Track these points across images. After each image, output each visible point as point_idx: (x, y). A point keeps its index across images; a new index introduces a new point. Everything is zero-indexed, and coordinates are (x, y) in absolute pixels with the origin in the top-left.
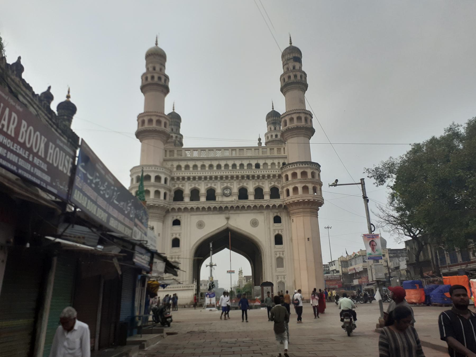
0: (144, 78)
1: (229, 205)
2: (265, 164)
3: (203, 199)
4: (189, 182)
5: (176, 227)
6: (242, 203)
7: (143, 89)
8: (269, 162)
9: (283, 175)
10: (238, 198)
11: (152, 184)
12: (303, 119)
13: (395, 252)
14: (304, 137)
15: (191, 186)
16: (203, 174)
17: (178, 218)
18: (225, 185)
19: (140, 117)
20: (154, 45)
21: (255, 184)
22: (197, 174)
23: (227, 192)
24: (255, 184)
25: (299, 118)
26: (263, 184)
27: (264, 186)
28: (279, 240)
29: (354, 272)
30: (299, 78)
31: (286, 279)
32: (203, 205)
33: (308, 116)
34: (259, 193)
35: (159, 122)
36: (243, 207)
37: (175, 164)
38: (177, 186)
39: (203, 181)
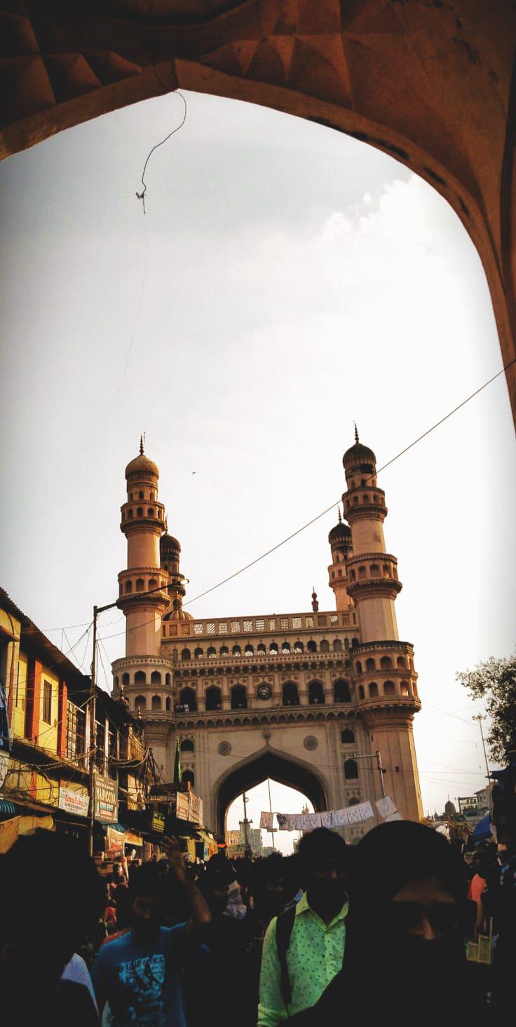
0: (125, 511)
1: (269, 715)
2: (324, 642)
6: (288, 710)
7: (124, 528)
17: (189, 737)
18: (261, 680)
19: (122, 576)
24: (309, 677)
25: (374, 568)
26: (321, 676)
27: (323, 680)
32: (226, 717)
34: (316, 690)
38: (184, 686)
39: (225, 675)
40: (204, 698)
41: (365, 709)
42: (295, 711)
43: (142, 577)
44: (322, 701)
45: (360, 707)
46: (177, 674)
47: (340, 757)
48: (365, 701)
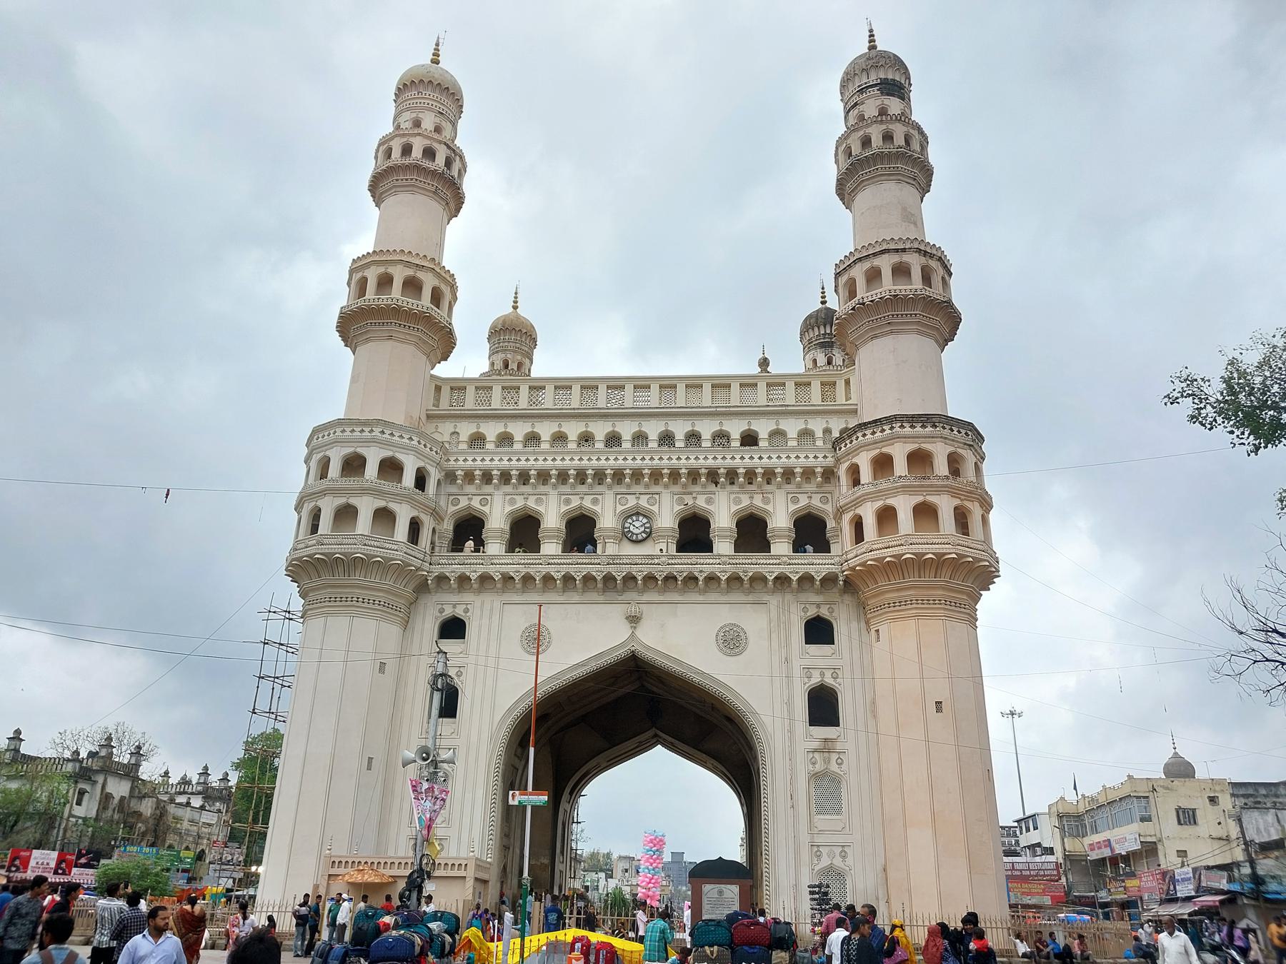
0: (380, 154)
1: (640, 572)
2: (778, 434)
3: (551, 548)
4: (508, 489)
5: (450, 645)
7: (379, 187)
8: (792, 427)
9: (842, 471)
11: (367, 485)
12: (916, 273)
13: (1251, 791)
15: (512, 502)
16: (553, 463)
17: (459, 612)
18: (632, 501)
20: (426, 59)
22: (534, 463)
23: (637, 527)
25: (901, 271)
27: (769, 508)
28: (823, 707)
29: (1106, 853)
30: (899, 140)
31: (849, 861)
32: (545, 569)
33: (934, 264)
34: (752, 532)
35: (413, 286)
37: (466, 429)
38: (464, 502)
40: (502, 531)
43: (391, 270)
44: (764, 546)
45: (852, 563)
47: (797, 672)
48: (863, 547)
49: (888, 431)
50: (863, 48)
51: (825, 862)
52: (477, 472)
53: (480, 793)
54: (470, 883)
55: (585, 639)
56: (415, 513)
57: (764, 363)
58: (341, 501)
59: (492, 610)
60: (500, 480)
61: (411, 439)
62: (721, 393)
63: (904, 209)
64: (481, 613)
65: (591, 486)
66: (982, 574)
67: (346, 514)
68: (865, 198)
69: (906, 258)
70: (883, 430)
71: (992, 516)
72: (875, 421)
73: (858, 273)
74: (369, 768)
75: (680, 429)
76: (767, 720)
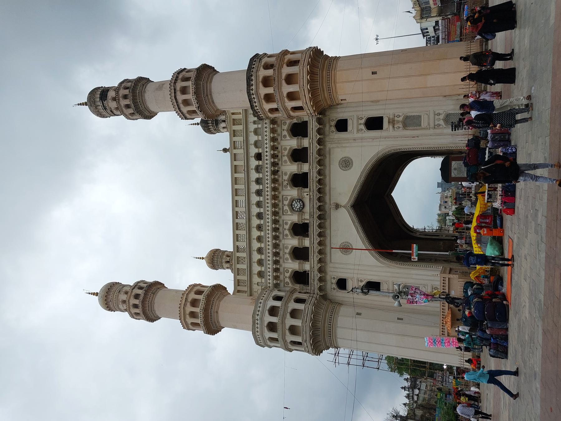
0: (138, 318)
1: (317, 204)
2: (256, 144)
3: (307, 242)
4: (281, 261)
5: (350, 285)
8: (253, 138)
10: (307, 190)
14: (211, 82)
15: (287, 259)
17: (334, 281)
18: (286, 208)
21: (285, 161)
22: (270, 250)
23: (297, 205)
24: (285, 161)
25: (184, 91)
27: (288, 148)
28: (374, 124)
30: (126, 92)
31: (441, 112)
32: (316, 245)
33: (180, 76)
34: (299, 155)
35: (194, 303)
36: (320, 182)
37: (256, 279)
41: (312, 106)
42: (313, 178)
43: (188, 312)
45: (312, 111)
46: (276, 286)
47: (360, 135)
48: (305, 106)
49: (254, 96)
50: (87, 107)
51: (442, 122)
52: (274, 274)
53: (413, 272)
54: (451, 276)
55: (345, 227)
56: (292, 301)
57: (225, 150)
58: (287, 332)
59: (334, 268)
60: (278, 265)
61: (260, 303)
62: (239, 169)
63: (157, 89)
64: (335, 271)
65: (280, 225)
66: (316, 53)
67: (293, 330)
68: (152, 107)
69: (178, 88)
70: (254, 98)
71: (291, 50)
72: (250, 102)
73: (185, 109)
74: (402, 319)
75: (255, 187)
76: (381, 148)
